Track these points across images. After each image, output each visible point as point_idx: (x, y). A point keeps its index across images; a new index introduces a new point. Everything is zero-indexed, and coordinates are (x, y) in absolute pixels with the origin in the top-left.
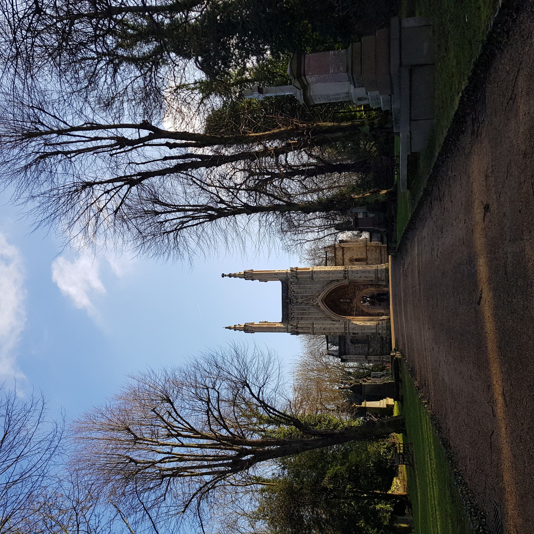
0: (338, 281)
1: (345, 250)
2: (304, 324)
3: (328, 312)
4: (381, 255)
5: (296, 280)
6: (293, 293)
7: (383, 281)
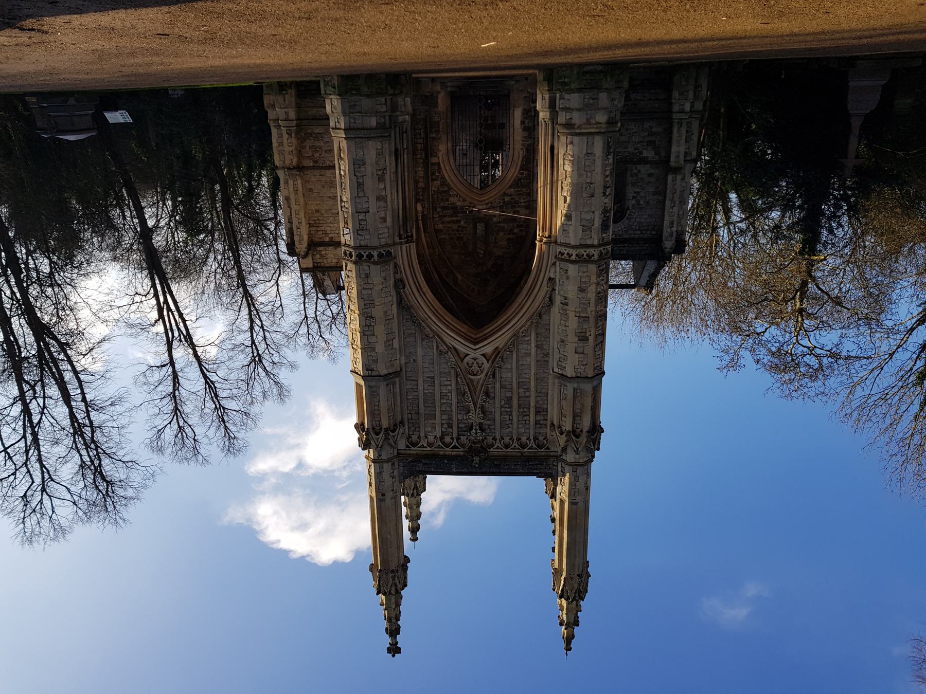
0: (399, 284)
1: (316, 239)
2: (561, 408)
3: (518, 318)
6: (447, 439)
7: (394, 108)
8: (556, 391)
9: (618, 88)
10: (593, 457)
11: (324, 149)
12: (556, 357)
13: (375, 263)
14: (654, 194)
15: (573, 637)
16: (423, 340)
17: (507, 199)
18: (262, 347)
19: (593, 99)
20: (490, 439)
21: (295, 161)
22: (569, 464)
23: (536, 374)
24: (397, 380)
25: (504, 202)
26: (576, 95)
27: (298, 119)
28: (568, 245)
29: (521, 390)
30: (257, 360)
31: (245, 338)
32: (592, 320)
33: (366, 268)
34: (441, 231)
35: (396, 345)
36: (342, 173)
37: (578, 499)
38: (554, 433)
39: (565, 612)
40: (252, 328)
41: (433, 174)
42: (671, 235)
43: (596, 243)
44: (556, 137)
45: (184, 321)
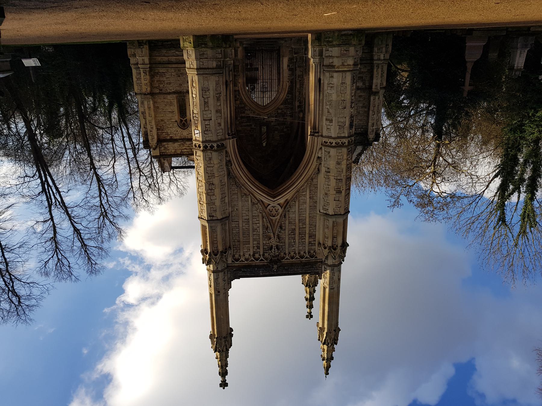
0: (229, 163)
1: (162, 137)
2: (324, 233)
3: (299, 182)
4: (170, 63)
5: (230, 252)
6: (257, 256)
8: (322, 223)
9: (360, 44)
10: (343, 261)
11: (166, 82)
12: (322, 203)
13: (215, 151)
14: (362, 107)
15: (330, 366)
16: (242, 196)
17: (280, 111)
18: (106, 207)
19: (346, 51)
20: (282, 254)
21: (149, 89)
22: (329, 266)
23: (309, 214)
24: (227, 221)
25: (278, 114)
26: (336, 48)
27: (150, 63)
28: (330, 137)
29: (301, 224)
30: (104, 215)
31: (96, 202)
32: (344, 180)
33: (209, 154)
35: (227, 201)
36: (194, 96)
37: (335, 286)
38: (320, 249)
39: (326, 352)
40: (100, 195)
42: (373, 131)
43: (347, 135)
44: (322, 73)
45: (59, 192)
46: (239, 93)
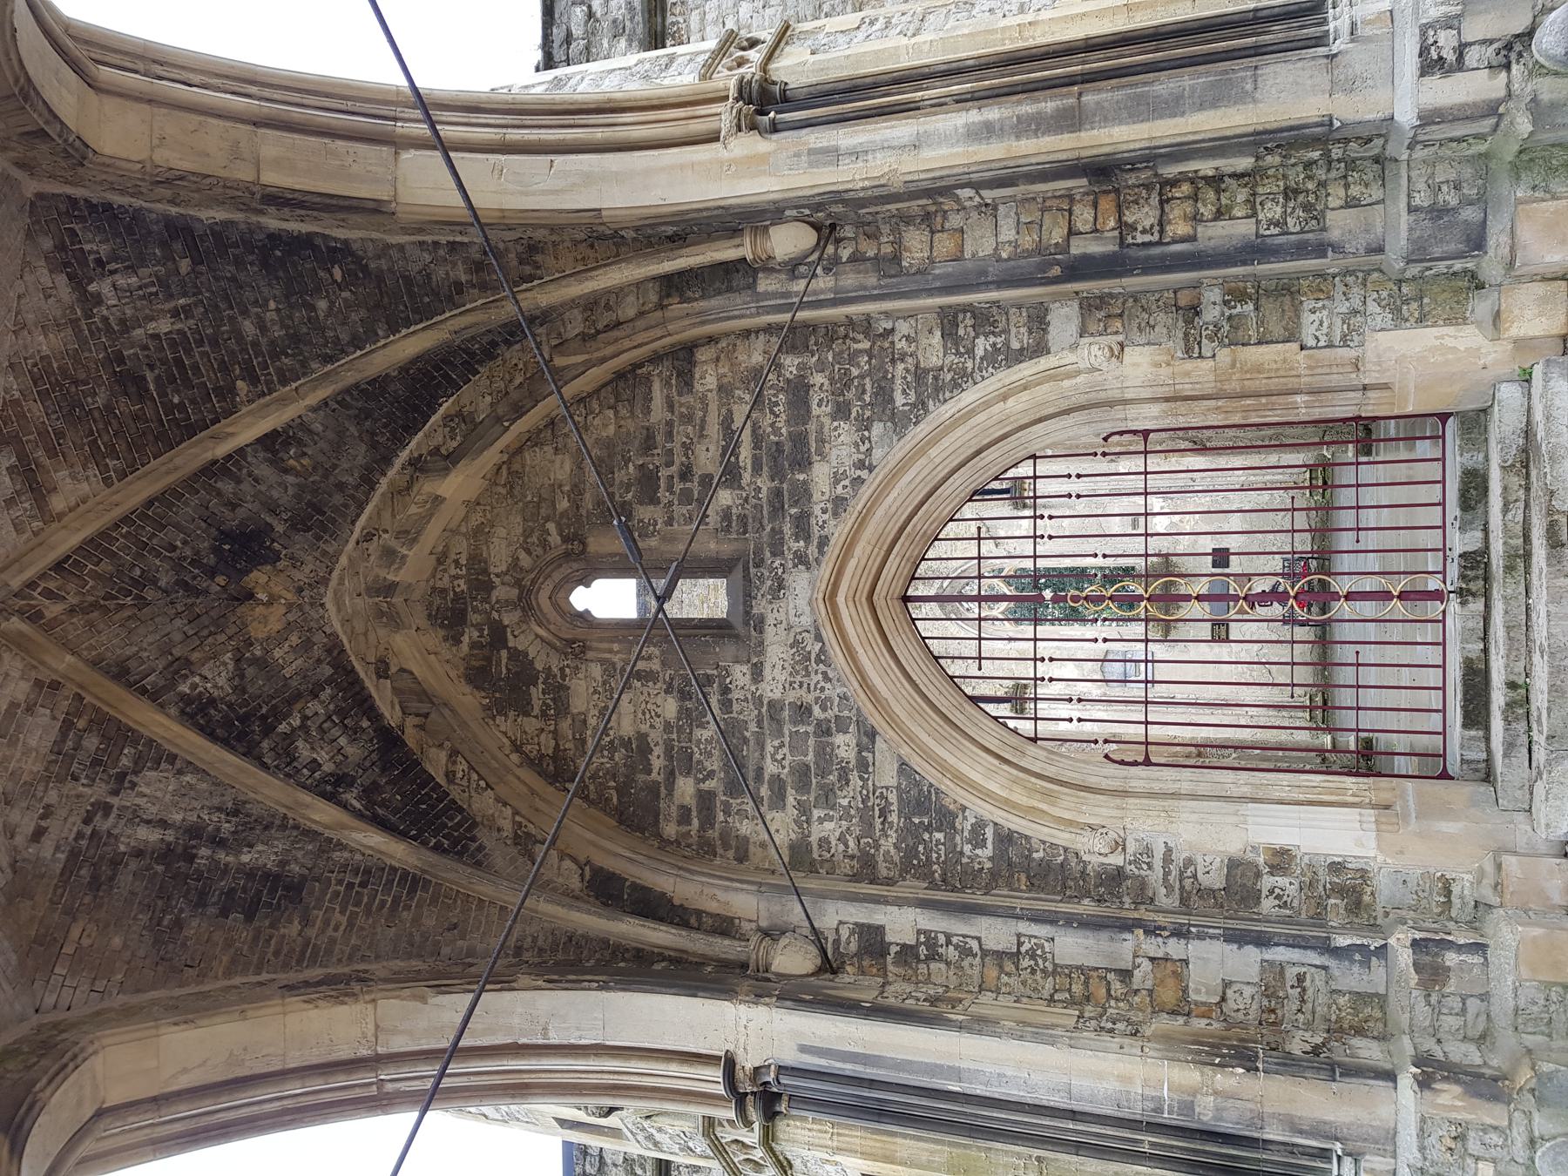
17: (845, 745)
25: (824, 730)
34: (686, 379)
41: (984, 320)
46: (1021, 356)
